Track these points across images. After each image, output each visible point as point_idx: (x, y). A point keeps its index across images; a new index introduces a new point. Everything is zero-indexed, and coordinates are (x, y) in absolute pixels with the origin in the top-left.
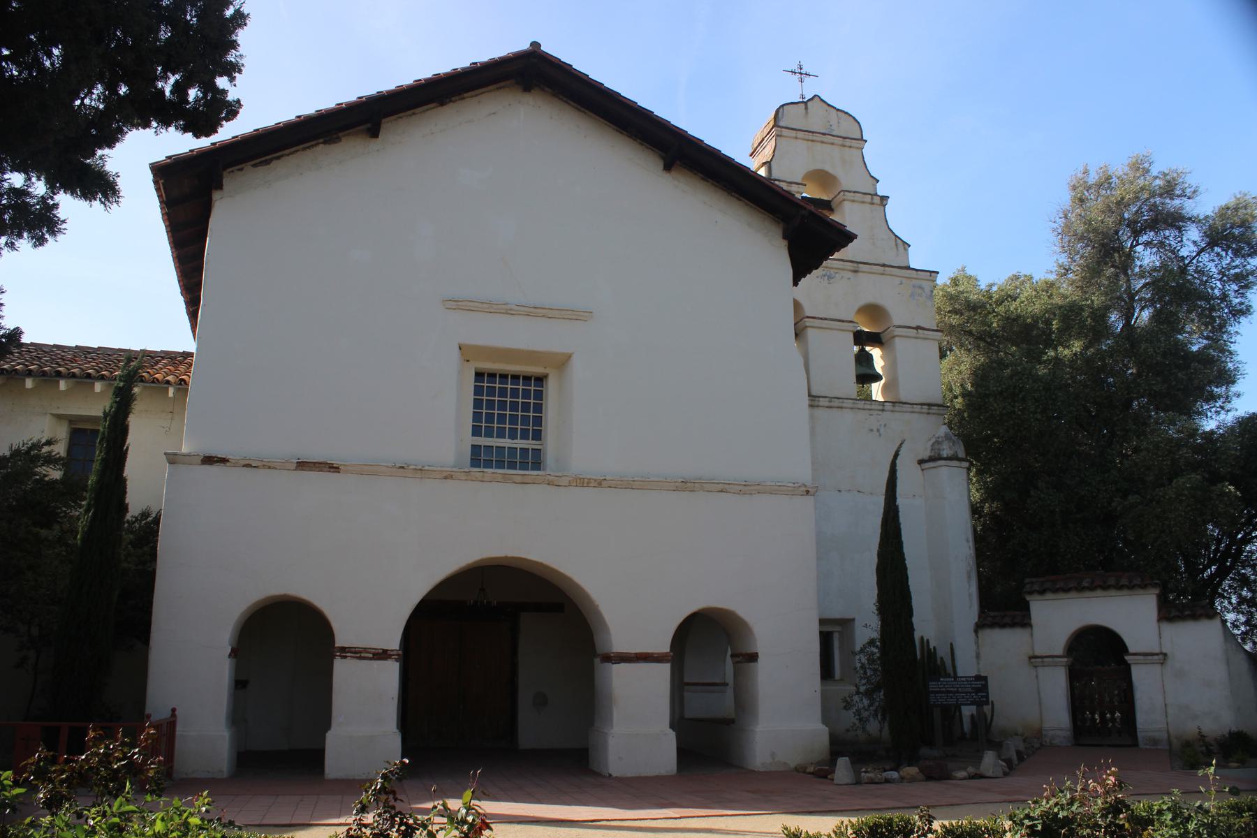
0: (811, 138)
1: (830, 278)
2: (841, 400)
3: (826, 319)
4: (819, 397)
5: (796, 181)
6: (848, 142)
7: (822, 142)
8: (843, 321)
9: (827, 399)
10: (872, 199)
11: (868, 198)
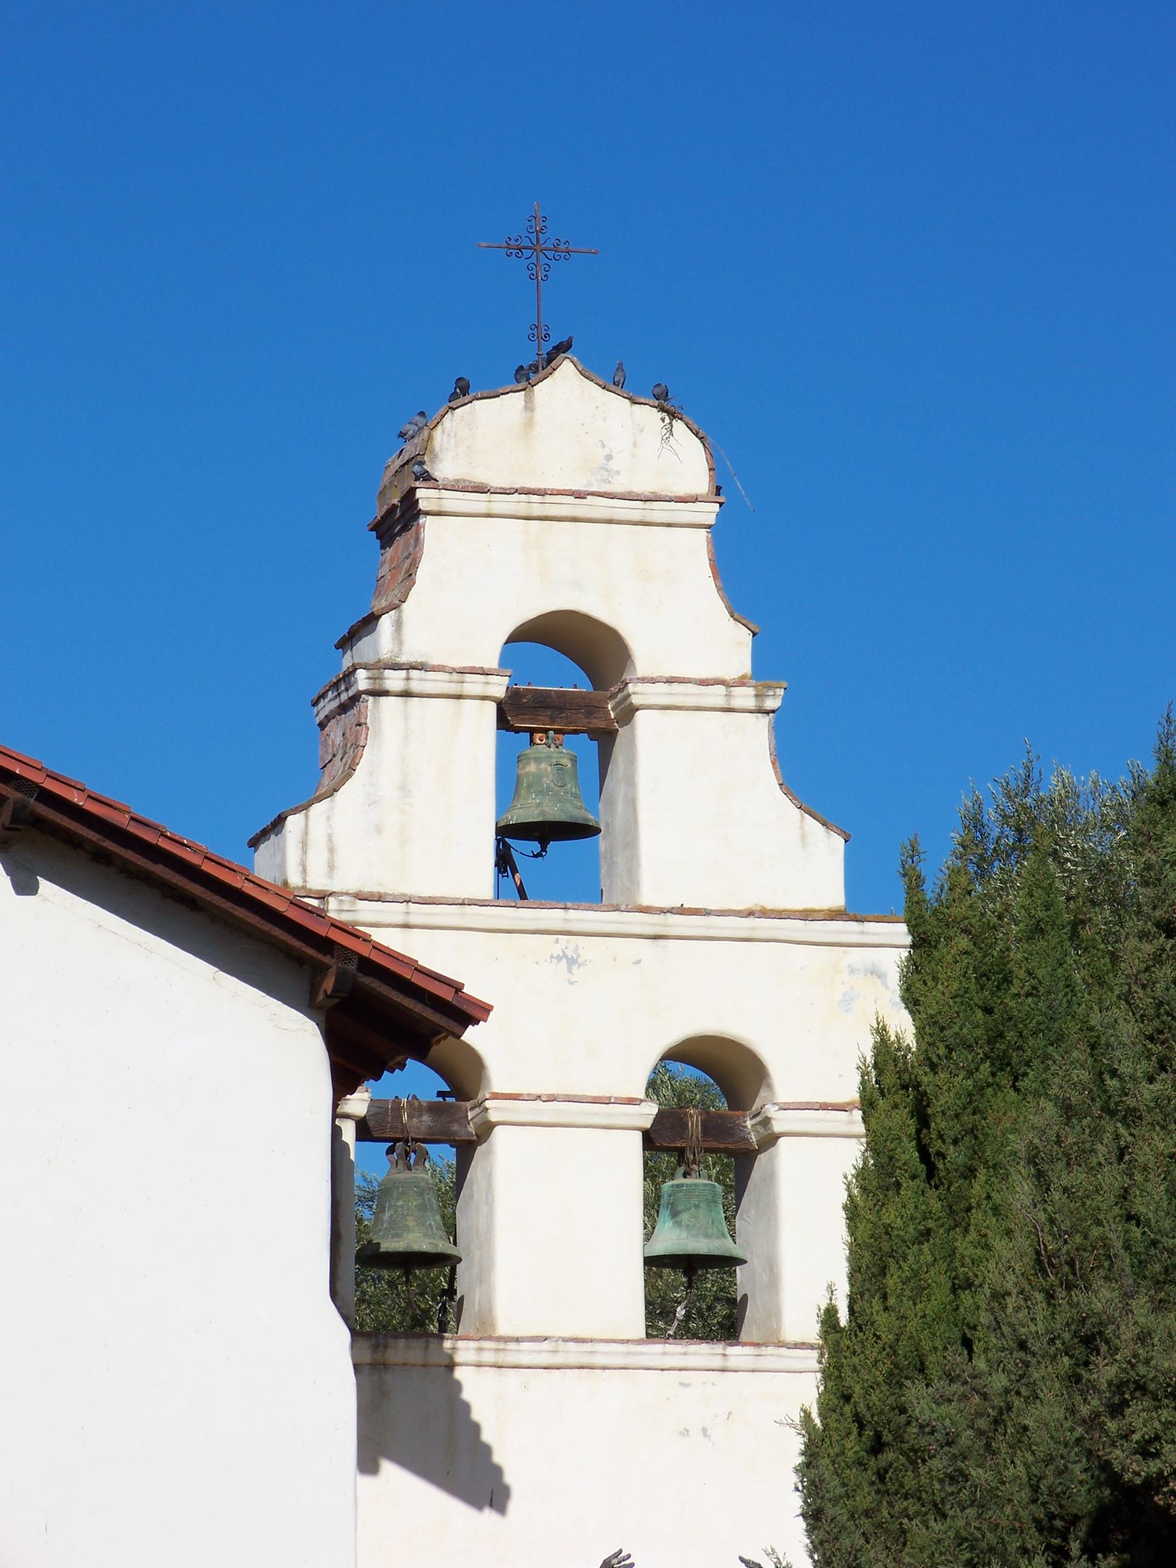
0: (537, 510)
1: (572, 962)
2: (587, 1347)
3: (552, 1098)
4: (517, 1340)
5: (478, 664)
6: (659, 511)
7: (575, 520)
8: (606, 1101)
9: (545, 1345)
10: (728, 695)
11: (716, 695)
